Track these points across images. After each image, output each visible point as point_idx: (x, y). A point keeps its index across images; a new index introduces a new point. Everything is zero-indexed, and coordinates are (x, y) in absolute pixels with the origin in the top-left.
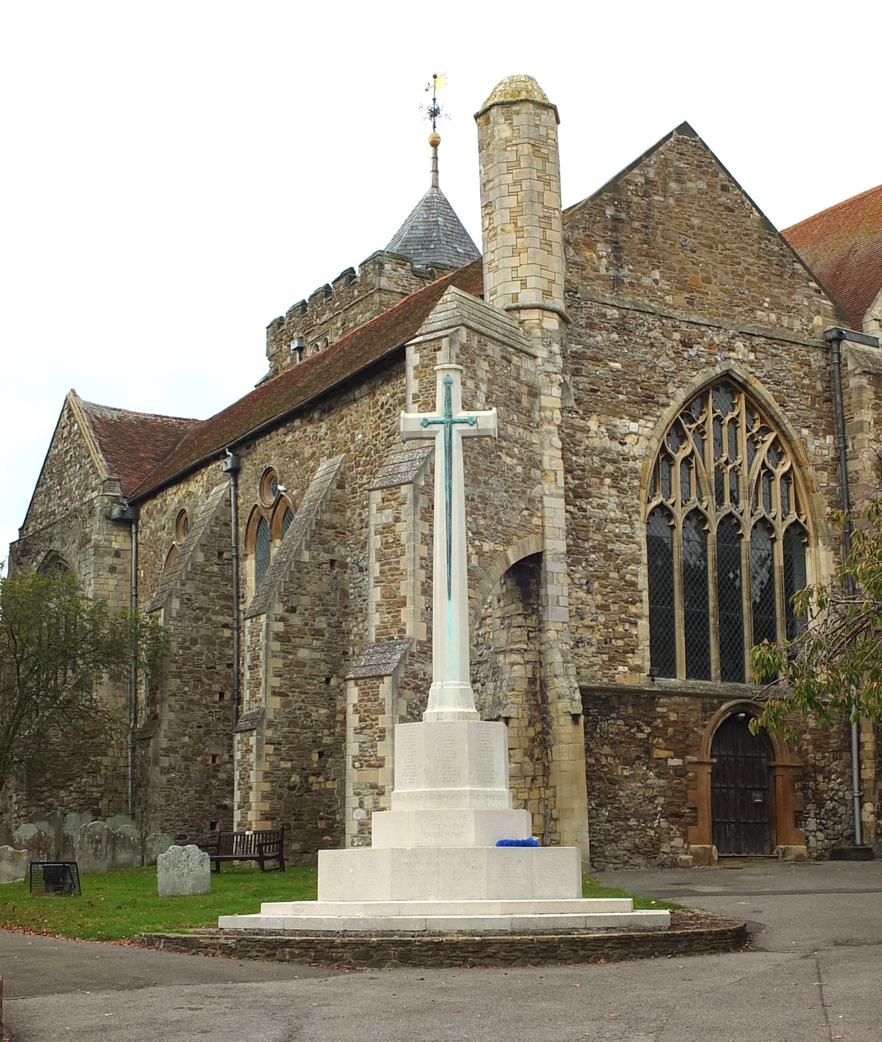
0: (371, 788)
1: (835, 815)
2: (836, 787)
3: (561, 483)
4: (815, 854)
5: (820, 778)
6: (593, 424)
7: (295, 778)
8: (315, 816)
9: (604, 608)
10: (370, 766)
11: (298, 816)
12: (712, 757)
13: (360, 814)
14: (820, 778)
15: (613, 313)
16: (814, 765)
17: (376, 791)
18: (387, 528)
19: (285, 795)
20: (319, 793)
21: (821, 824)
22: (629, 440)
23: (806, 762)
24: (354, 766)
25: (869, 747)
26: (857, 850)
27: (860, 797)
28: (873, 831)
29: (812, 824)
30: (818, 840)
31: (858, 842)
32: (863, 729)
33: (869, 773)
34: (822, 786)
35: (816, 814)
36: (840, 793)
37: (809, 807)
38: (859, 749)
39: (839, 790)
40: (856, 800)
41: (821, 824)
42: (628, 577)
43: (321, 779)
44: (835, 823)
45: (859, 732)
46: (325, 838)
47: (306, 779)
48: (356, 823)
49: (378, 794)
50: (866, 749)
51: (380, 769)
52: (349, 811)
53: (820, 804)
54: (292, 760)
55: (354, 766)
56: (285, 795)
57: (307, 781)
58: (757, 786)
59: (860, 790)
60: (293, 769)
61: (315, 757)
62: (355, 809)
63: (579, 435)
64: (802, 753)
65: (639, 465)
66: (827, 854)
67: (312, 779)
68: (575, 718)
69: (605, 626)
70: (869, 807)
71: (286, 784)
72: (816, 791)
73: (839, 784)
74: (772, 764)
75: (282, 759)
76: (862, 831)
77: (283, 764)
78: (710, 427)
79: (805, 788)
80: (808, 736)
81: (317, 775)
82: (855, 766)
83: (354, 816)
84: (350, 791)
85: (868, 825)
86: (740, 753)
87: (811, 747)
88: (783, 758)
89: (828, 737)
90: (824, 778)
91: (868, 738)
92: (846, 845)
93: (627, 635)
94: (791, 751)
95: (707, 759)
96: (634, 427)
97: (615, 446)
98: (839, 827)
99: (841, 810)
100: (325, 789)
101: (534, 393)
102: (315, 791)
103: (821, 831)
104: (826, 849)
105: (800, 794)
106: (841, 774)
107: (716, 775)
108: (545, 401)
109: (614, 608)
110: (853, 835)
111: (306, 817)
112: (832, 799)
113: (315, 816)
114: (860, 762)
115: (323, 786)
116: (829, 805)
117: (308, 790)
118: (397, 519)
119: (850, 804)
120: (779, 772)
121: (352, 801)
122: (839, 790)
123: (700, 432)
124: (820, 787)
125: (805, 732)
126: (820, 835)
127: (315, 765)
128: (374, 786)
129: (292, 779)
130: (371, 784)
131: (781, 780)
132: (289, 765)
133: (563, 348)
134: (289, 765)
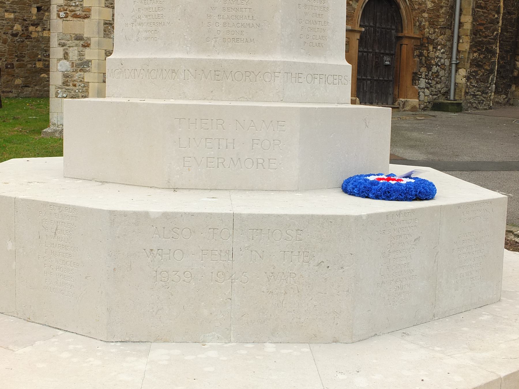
0: (76, 39)
1: (437, 76)
2: (440, 56)
4: (422, 106)
5: (431, 48)
7: (17, 27)
8: (34, 58)
10: (76, 16)
11: (20, 58)
12: (361, 26)
13: (64, 66)
14: (431, 48)
16: (428, 38)
17: (82, 42)
19: (9, 40)
20: (38, 40)
21: (429, 83)
23: (423, 35)
24: (58, 16)
25: (468, 26)
26: (452, 104)
27: (457, 64)
28: (463, 91)
29: (423, 83)
30: (426, 96)
31: (452, 98)
32: (464, 12)
33: (465, 46)
34: (432, 54)
35: (426, 75)
36: (442, 60)
37: (423, 69)
38: (459, 28)
39: (441, 58)
40: (454, 67)
41: (429, 83)
43: (39, 29)
44: (437, 83)
45: (460, 14)
46: (42, 75)
47: (27, 28)
48: (60, 75)
49: (83, 46)
50: (464, 28)
51: (86, 20)
52: (53, 62)
53: (429, 69)
54: (14, 12)
55: (58, 16)
56: (9, 40)
57: (27, 30)
58: (387, 52)
59: (457, 59)
60: (16, 20)
61: (34, 11)
62: (59, 60)
64: (421, 28)
66: (430, 106)
67: (31, 28)
70: (463, 72)
71: (10, 31)
72: (427, 58)
73: (442, 53)
74: (400, 35)
75: (6, 11)
76: (455, 89)
77: (7, 15)
79: (421, 55)
80: (426, 15)
81: (36, 25)
82: (455, 40)
83: (59, 68)
84: (54, 42)
85: (460, 86)
86: (378, 25)
87: (427, 24)
88: (409, 31)
89: (438, 16)
90: (434, 48)
91: (468, 20)
92: (442, 100)
94: (415, 25)
95: (357, 28)
98: (439, 86)
99: (442, 73)
100: (43, 37)
102: (34, 38)
103: (427, 88)
104: (429, 102)
105: (417, 59)
106: (444, 46)
107: (361, 41)
110: (447, 93)
111: (26, 59)
112: (437, 65)
113: (34, 58)
114: (459, 37)
115: (40, 34)
116: (435, 69)
117: (28, 37)
119: (447, 69)
120: (405, 41)
121: (56, 52)
122: (441, 58)
124: (430, 55)
125: (424, 11)
126: (427, 92)
127: (34, 17)
128: (79, 38)
129: (15, 28)
130: (76, 35)
131: (407, 47)
132: (12, 16)
134: (12, 16)
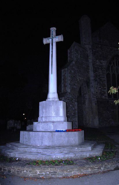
3: (93, 69)
6: (97, 61)
9: (100, 87)
15: (100, 46)
18: (64, 75)
22: (103, 63)
42: (104, 83)
63: (95, 63)
65: (105, 67)
68: (96, 104)
69: (100, 90)
78: (115, 62)
93: (104, 91)
96: (104, 62)
97: (101, 64)
101: (88, 56)
108: (89, 58)
109: (102, 87)
118: (65, 74)
123: (114, 63)
133: (92, 51)
